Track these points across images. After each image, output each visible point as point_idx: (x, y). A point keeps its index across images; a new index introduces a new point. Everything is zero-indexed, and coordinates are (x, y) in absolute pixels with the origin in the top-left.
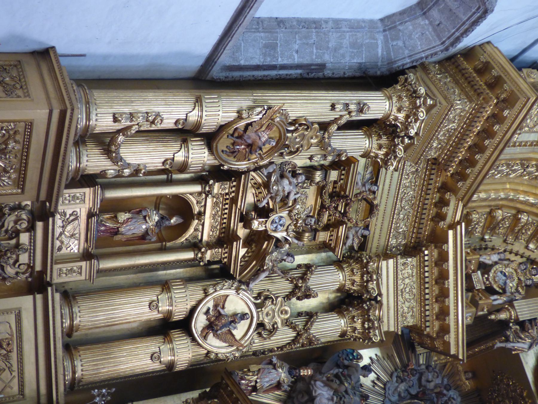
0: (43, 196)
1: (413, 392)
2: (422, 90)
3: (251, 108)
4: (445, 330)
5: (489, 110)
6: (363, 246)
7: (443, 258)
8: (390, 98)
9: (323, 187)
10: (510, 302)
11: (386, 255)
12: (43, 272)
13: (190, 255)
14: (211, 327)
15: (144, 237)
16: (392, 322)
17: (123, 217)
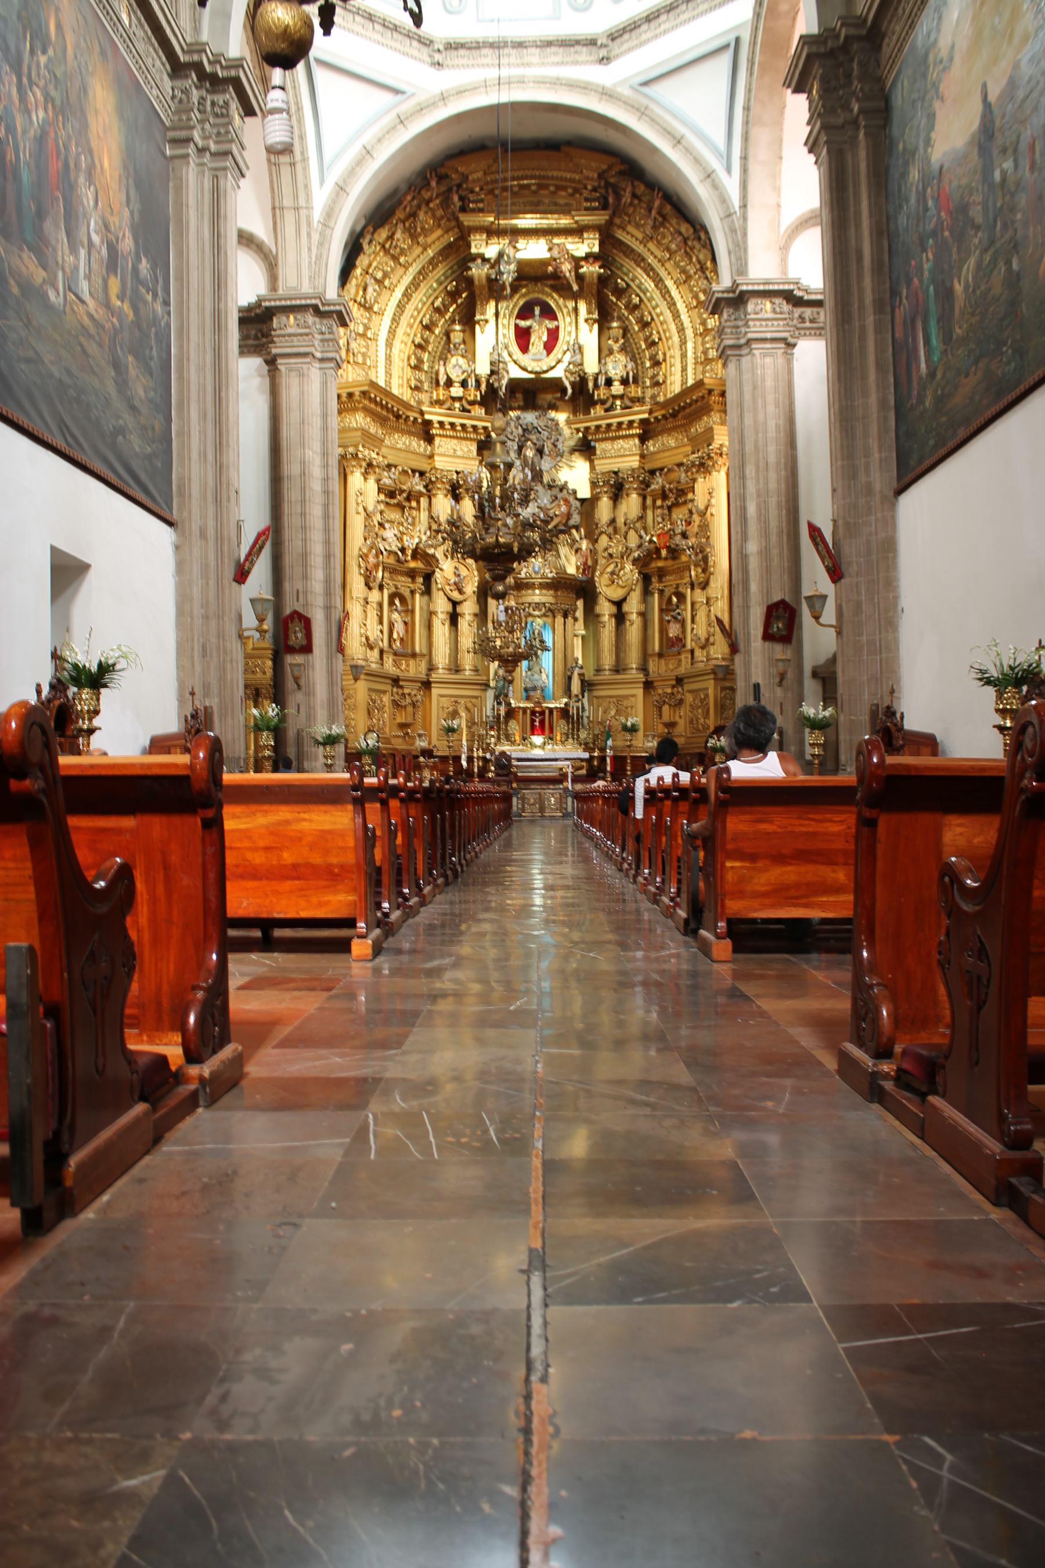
0: (390, 681)
1: (516, 447)
2: (351, 450)
3: (360, 566)
4: (485, 428)
5: (366, 402)
6: (422, 474)
7: (441, 423)
8: (352, 472)
9: (387, 504)
10: (476, 376)
11: (431, 457)
12: (423, 683)
13: (417, 596)
14: (461, 592)
15: (406, 623)
16: (473, 462)
17: (395, 636)
